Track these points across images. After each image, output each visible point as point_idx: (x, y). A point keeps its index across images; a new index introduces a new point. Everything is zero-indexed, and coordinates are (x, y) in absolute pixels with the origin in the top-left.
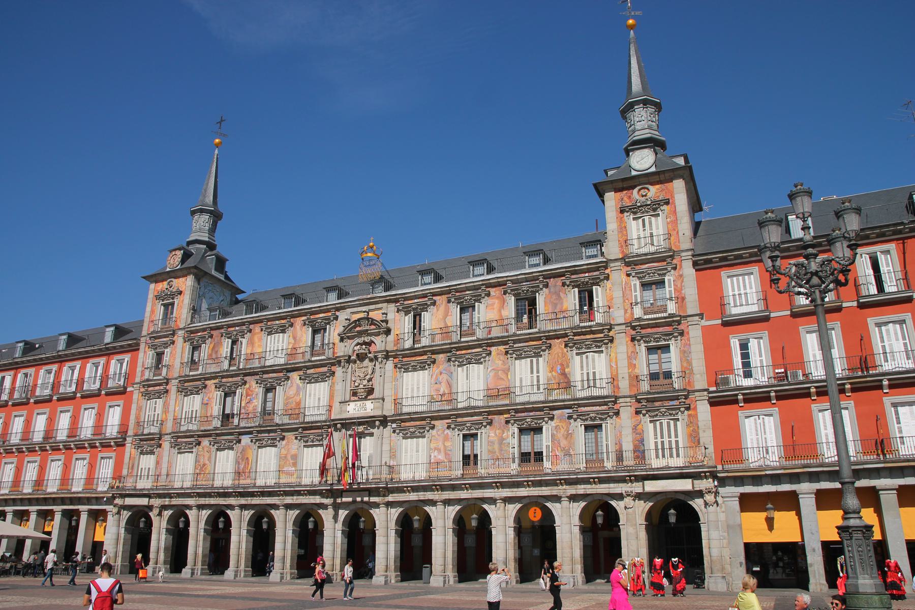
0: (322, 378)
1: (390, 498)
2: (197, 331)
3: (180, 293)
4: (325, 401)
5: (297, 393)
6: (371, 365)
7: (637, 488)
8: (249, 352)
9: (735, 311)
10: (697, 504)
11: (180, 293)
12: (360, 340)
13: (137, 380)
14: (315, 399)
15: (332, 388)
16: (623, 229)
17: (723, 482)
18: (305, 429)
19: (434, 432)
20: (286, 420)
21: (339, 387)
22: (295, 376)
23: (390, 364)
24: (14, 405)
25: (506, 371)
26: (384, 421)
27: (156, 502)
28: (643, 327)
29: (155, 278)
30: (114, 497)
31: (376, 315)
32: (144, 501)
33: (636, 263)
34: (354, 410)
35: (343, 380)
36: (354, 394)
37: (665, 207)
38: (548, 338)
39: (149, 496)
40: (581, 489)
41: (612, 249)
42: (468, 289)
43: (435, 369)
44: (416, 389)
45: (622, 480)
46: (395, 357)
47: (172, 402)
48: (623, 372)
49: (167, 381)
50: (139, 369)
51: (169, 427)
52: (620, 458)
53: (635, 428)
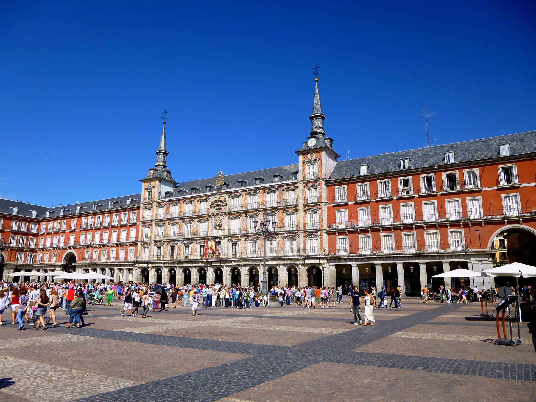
0: (205, 221)
1: (227, 264)
3: (154, 187)
4: (206, 230)
5: (197, 226)
6: (221, 217)
7: (303, 262)
9: (338, 201)
10: (321, 268)
11: (154, 187)
12: (217, 208)
13: (141, 220)
14: (203, 229)
15: (208, 225)
16: (304, 169)
17: (328, 261)
18: (199, 239)
19: (241, 241)
21: (210, 224)
22: (196, 220)
23: (227, 216)
24: (95, 229)
26: (225, 237)
27: (150, 265)
28: (308, 206)
29: (144, 181)
30: (135, 264)
31: (222, 199)
32: (146, 265)
33: (307, 183)
34: (215, 233)
35: (212, 222)
36: (215, 227)
37: (318, 162)
38: (278, 209)
39: (147, 263)
40: (286, 262)
41: (300, 177)
42: (253, 190)
43: (241, 219)
44: (235, 226)
45: (298, 259)
46: (229, 214)
47: (154, 229)
48: (301, 222)
49: (151, 221)
50: (141, 216)
51: (153, 239)
52: (299, 252)
53: (304, 241)
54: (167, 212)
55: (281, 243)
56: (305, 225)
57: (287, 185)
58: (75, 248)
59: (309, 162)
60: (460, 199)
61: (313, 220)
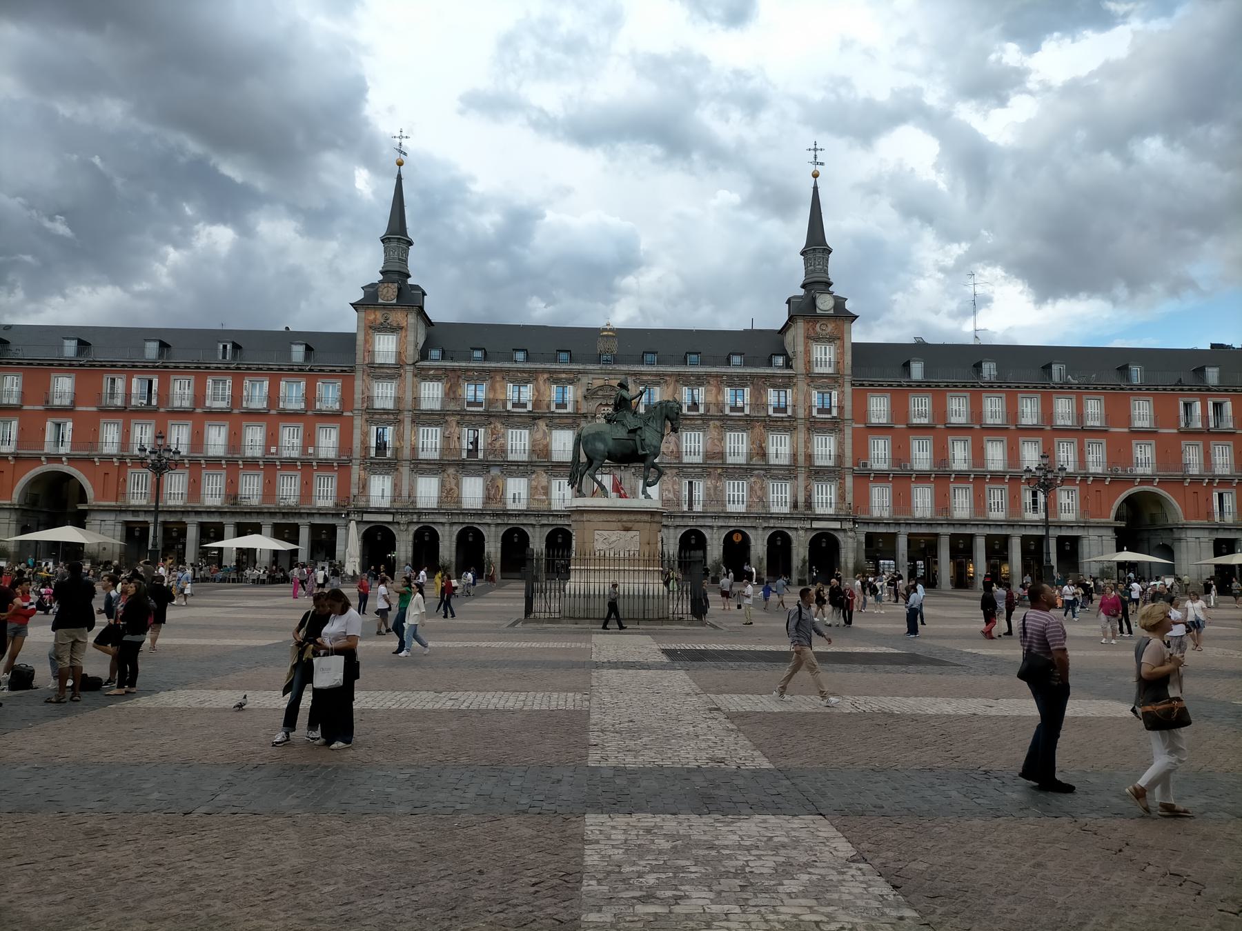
2: (430, 369)
3: (402, 328)
8: (491, 396)
10: (840, 537)
13: (358, 405)
16: (808, 352)
20: (535, 458)
22: (542, 424)
25: (722, 440)
27: (403, 519)
30: (348, 514)
32: (389, 518)
41: (799, 365)
48: (801, 450)
50: (358, 396)
51: (406, 453)
52: (795, 505)
54: (451, 394)
55: (757, 487)
56: (809, 457)
57: (773, 376)
58: (72, 460)
59: (818, 339)
60: (1076, 441)
61: (824, 448)
